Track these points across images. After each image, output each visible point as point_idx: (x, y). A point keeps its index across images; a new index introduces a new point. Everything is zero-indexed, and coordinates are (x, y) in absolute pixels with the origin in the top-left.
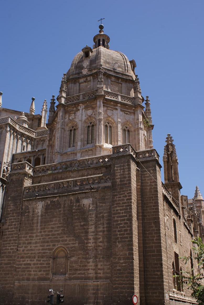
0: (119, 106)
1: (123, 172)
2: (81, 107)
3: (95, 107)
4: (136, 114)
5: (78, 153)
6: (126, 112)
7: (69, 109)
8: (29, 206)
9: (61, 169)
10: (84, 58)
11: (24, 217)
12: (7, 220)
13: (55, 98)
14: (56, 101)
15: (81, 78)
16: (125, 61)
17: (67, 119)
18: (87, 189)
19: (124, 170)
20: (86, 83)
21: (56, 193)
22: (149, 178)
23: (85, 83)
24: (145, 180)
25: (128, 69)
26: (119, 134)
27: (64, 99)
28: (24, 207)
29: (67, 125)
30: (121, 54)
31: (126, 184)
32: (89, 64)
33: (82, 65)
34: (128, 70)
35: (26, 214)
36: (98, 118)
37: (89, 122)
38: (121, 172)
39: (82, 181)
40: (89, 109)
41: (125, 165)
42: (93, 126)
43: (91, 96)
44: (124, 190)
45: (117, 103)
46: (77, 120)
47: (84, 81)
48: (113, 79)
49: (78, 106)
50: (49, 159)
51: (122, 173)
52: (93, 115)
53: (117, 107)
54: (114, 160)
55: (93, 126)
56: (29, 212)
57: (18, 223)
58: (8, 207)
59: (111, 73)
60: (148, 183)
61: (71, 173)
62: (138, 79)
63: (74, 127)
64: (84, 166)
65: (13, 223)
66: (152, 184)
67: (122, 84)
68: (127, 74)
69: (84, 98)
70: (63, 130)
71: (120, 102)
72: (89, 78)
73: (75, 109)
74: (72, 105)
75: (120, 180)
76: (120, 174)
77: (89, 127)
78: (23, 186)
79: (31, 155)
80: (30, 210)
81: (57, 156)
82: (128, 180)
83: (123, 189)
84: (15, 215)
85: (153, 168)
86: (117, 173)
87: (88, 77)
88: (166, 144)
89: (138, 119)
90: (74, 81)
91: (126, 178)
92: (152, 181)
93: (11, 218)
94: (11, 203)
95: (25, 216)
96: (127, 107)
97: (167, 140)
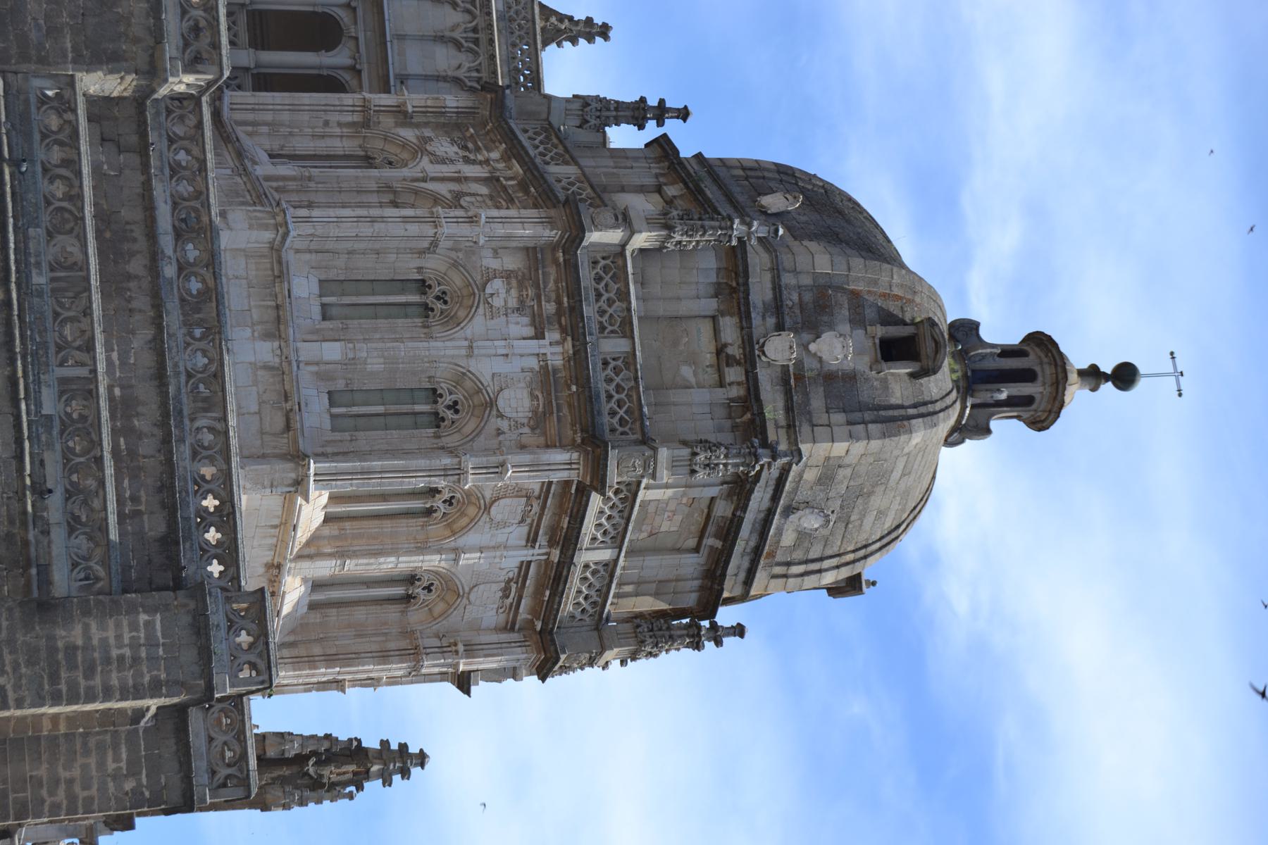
0: (548, 554)
1: (121, 658)
2: (554, 350)
3: (545, 434)
4: (504, 637)
5: (276, 344)
6: (514, 586)
7: (552, 271)
9: (181, 269)
10: (880, 331)
13: (672, 127)
14: (652, 131)
15: (742, 329)
16: (850, 557)
17: (494, 264)
18: (42, 463)
19: (131, 667)
20: (709, 358)
21: (29, 277)
22: (94, 773)
23: (712, 348)
24: (86, 752)
25: (791, 580)
26: (382, 560)
27: (617, 242)
29: (455, 265)
30: (898, 526)
31: (54, 678)
32: (834, 368)
33: (831, 327)
34: (785, 576)
36: (470, 463)
37: (458, 396)
38: (119, 647)
39: (87, 427)
40: (533, 397)
41: (159, 670)
42: (437, 420)
43: (613, 404)
44: (24, 670)
45: (568, 541)
46: (478, 324)
47: (725, 345)
48: (723, 509)
49: (563, 330)
50: (285, 117)
51: (115, 653)
52: (495, 423)
53: (542, 539)
54: (192, 605)
55: (437, 420)
59: (759, 498)
60: (67, 767)
61: (147, 333)
62: (718, 643)
63: (439, 306)
64: (178, 408)
66: (62, 787)
67: (697, 550)
68: (761, 577)
69: (606, 363)
70: (426, 245)
71: (571, 563)
72: (734, 374)
73: (550, 308)
74: (575, 292)
75: (75, 648)
76: (112, 641)
77: (434, 394)
78: (80, 71)
81: (266, 227)
82: (73, 686)
83: (30, 663)
85: (147, 794)
86: (118, 625)
87: (747, 372)
88: (371, 743)
89: (471, 650)
90: (734, 284)
91: (86, 678)
92: (77, 788)
96: (548, 593)
97: (394, 746)
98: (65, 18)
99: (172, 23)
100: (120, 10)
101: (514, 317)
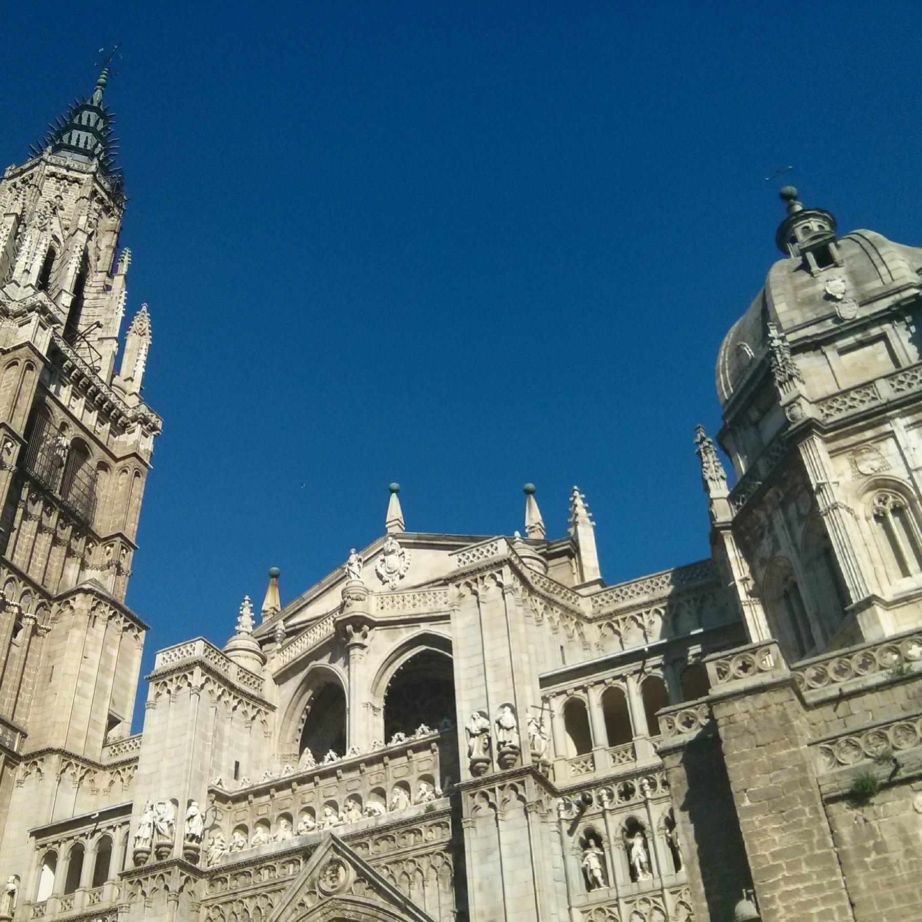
8: (874, 824)
11: (859, 874)
12: (771, 900)
17: (848, 475)
28: (845, 831)
35: (867, 859)
56: (880, 847)
57: (840, 903)
58: (756, 843)
65: (814, 911)
73: (869, 434)
79: (617, 671)
80: (886, 837)
84: (805, 870)
93: (791, 887)
94: (762, 822)
95: (863, 865)
98: (764, 759)
99: (749, 681)
100: (746, 722)
101: (883, 452)
